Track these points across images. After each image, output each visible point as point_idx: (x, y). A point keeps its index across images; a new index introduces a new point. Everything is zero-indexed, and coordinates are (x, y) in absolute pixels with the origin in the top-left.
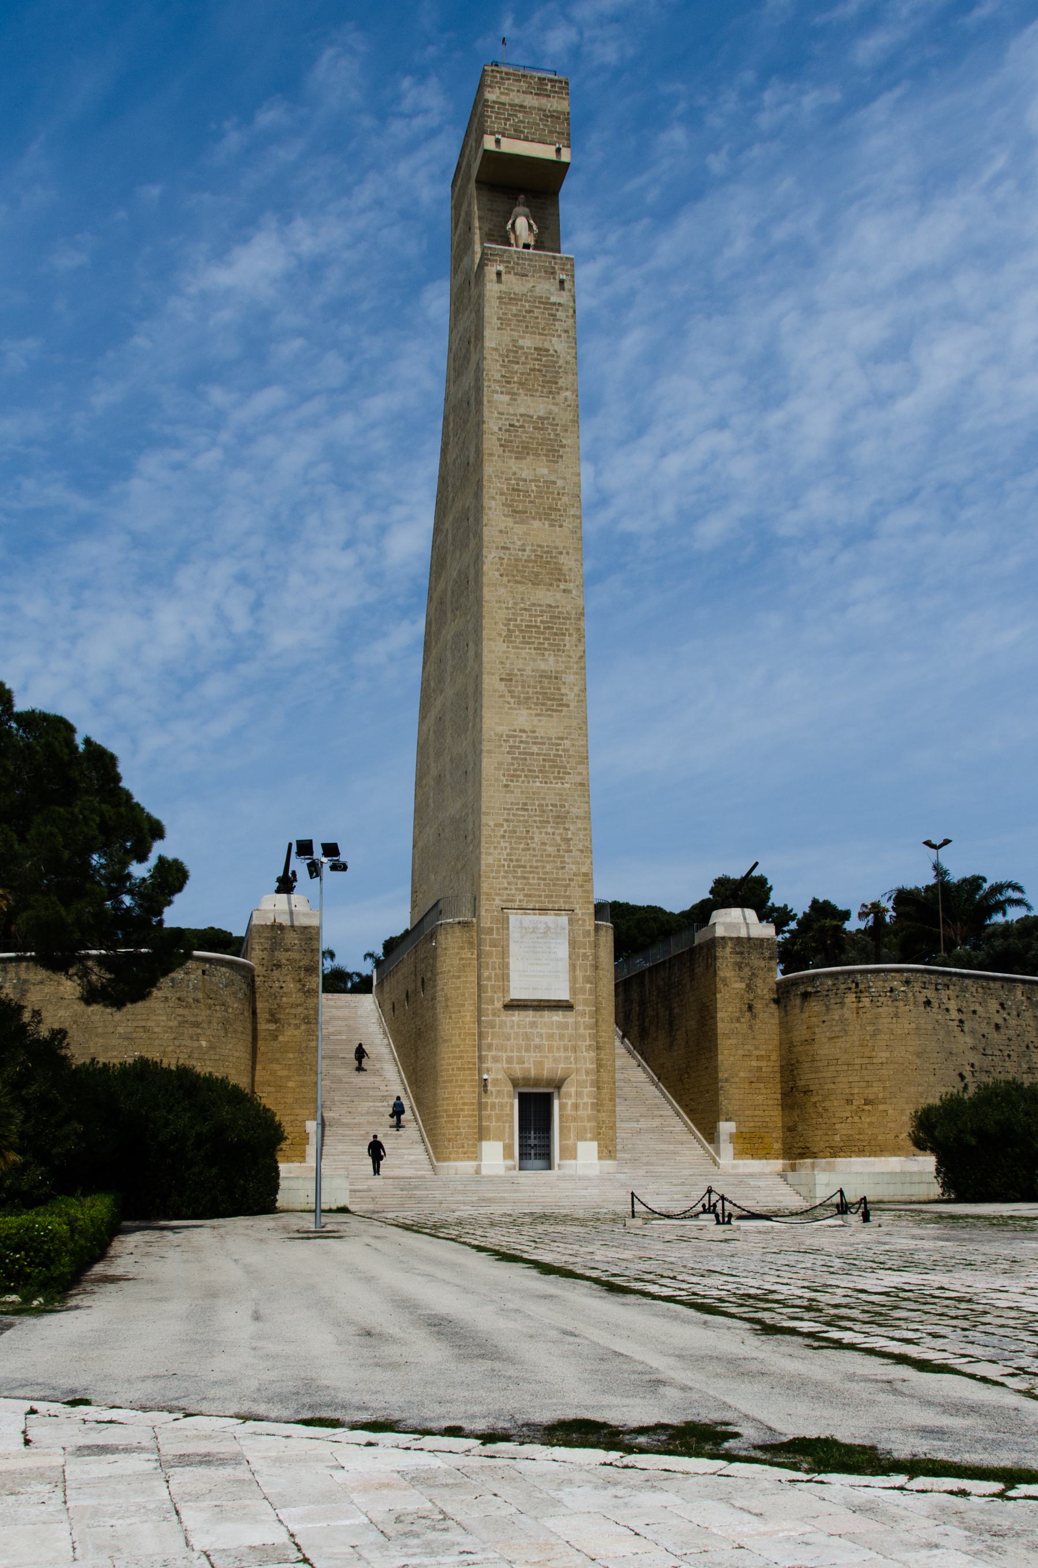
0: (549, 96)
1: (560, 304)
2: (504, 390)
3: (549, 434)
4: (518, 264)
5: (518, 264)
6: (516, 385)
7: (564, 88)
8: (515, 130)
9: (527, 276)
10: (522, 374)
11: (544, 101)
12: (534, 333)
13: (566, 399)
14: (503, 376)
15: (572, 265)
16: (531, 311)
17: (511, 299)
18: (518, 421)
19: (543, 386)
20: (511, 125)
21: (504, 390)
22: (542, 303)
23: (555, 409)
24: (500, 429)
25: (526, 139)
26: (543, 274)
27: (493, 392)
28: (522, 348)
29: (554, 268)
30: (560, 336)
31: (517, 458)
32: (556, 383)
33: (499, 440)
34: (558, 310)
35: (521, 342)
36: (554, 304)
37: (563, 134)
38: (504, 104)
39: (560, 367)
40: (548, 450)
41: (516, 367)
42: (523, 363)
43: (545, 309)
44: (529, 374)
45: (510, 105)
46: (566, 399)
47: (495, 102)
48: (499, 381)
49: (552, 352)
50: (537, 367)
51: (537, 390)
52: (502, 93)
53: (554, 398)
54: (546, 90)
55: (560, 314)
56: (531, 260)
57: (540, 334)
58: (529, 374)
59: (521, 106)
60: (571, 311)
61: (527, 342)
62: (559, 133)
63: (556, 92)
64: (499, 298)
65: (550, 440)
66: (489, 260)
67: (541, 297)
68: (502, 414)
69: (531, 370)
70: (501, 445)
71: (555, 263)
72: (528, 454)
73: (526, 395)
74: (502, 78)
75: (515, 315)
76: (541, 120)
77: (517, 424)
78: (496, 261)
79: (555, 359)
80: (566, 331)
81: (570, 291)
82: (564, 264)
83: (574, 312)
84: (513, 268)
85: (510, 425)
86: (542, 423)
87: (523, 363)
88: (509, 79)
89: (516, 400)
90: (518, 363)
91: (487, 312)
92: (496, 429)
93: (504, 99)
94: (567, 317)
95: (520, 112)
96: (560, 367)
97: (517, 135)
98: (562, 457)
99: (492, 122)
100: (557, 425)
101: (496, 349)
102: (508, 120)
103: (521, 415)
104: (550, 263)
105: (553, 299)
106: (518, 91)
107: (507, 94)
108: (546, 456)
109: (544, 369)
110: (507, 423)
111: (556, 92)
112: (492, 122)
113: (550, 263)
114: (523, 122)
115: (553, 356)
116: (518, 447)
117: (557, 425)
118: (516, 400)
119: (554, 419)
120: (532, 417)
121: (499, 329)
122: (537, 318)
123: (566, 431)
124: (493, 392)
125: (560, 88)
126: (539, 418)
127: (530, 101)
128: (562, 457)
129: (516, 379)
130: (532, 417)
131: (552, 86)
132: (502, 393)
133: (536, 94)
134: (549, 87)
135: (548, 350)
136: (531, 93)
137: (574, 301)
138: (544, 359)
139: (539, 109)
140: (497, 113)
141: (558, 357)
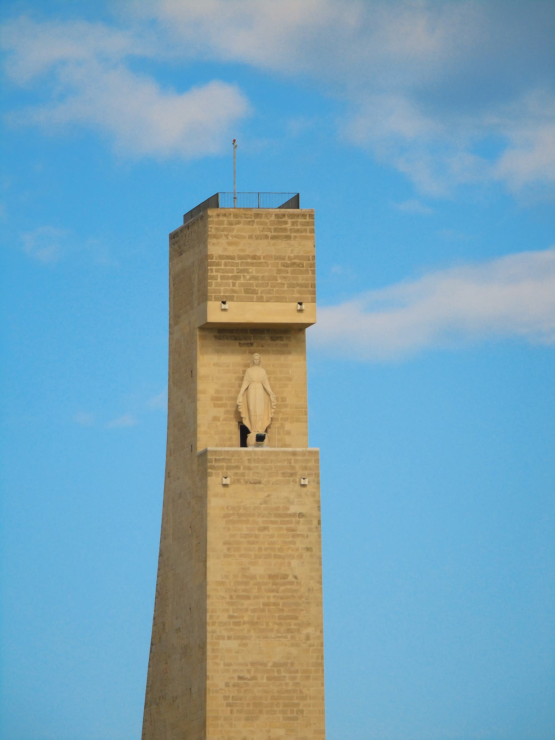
0: (288, 237)
1: (301, 515)
2: (232, 633)
3: (287, 684)
4: (249, 469)
5: (249, 469)
6: (246, 627)
7: (308, 224)
8: (246, 291)
9: (260, 483)
10: (254, 611)
11: (282, 245)
12: (268, 557)
13: (308, 638)
14: (231, 617)
15: (317, 461)
16: (265, 528)
17: (240, 515)
18: (249, 671)
19: (280, 624)
20: (241, 285)
21: (232, 633)
22: (279, 516)
23: (294, 651)
24: (227, 685)
25: (260, 299)
26: (280, 478)
27: (219, 638)
28: (254, 577)
29: (293, 468)
30: (300, 557)
31: (247, 719)
32: (296, 618)
33: (226, 698)
34: (298, 523)
35: (253, 570)
36: (294, 515)
37: (306, 286)
38: (232, 258)
39: (301, 597)
40: (285, 705)
41: (247, 602)
42: (256, 597)
43: (283, 523)
44: (263, 611)
45: (240, 258)
46: (308, 638)
47: (221, 257)
48: (225, 624)
49: (291, 578)
50: (272, 600)
51: (272, 630)
52: (230, 244)
53: (293, 637)
54: (285, 230)
55: (302, 528)
56: (264, 461)
57: (276, 556)
58: (263, 611)
59: (254, 257)
60: (315, 522)
61: (259, 570)
62: (301, 286)
63: (298, 231)
64: (226, 516)
65: (288, 691)
66: (213, 467)
67: (277, 509)
68: (230, 665)
69: (266, 605)
70: (228, 705)
71: (296, 461)
72: (260, 712)
73: (259, 637)
74: (230, 224)
75: (246, 536)
76: (279, 271)
77: (248, 676)
78: (221, 468)
79: (295, 587)
80: (308, 549)
81: (314, 495)
82: (307, 461)
83: (319, 523)
84: (243, 475)
85: (240, 678)
86: (279, 672)
87: (256, 597)
88: (238, 223)
89: (245, 645)
90: (248, 598)
91: (211, 536)
92: (222, 685)
93: (232, 251)
94: (310, 530)
95: (252, 264)
96: (301, 597)
97: (250, 294)
98: (302, 712)
99: (217, 283)
100: (297, 671)
101: (222, 583)
102: (236, 278)
103: (253, 664)
104: (289, 461)
105: (293, 509)
106: (250, 237)
107: (235, 244)
108: (283, 712)
109: (281, 602)
110: (236, 675)
111: (298, 231)
112: (217, 284)
113: (289, 461)
114: (256, 278)
115: (292, 583)
116: (248, 705)
117: (297, 671)
118: (245, 645)
119: (292, 664)
120: (265, 665)
121: (226, 556)
122: (272, 536)
123: (308, 678)
124: (219, 638)
125: (303, 224)
126: (275, 665)
127: (263, 248)
128: (302, 712)
129: (246, 619)
130: (265, 665)
131: (293, 224)
132: (229, 638)
133: (273, 238)
134: (289, 226)
135: (285, 576)
136: (266, 237)
137: (319, 510)
138: (282, 588)
139: (277, 258)
140: (224, 271)
141: (299, 584)
